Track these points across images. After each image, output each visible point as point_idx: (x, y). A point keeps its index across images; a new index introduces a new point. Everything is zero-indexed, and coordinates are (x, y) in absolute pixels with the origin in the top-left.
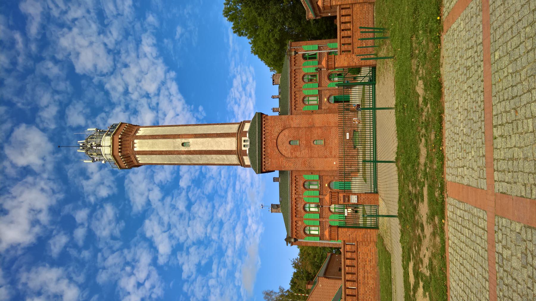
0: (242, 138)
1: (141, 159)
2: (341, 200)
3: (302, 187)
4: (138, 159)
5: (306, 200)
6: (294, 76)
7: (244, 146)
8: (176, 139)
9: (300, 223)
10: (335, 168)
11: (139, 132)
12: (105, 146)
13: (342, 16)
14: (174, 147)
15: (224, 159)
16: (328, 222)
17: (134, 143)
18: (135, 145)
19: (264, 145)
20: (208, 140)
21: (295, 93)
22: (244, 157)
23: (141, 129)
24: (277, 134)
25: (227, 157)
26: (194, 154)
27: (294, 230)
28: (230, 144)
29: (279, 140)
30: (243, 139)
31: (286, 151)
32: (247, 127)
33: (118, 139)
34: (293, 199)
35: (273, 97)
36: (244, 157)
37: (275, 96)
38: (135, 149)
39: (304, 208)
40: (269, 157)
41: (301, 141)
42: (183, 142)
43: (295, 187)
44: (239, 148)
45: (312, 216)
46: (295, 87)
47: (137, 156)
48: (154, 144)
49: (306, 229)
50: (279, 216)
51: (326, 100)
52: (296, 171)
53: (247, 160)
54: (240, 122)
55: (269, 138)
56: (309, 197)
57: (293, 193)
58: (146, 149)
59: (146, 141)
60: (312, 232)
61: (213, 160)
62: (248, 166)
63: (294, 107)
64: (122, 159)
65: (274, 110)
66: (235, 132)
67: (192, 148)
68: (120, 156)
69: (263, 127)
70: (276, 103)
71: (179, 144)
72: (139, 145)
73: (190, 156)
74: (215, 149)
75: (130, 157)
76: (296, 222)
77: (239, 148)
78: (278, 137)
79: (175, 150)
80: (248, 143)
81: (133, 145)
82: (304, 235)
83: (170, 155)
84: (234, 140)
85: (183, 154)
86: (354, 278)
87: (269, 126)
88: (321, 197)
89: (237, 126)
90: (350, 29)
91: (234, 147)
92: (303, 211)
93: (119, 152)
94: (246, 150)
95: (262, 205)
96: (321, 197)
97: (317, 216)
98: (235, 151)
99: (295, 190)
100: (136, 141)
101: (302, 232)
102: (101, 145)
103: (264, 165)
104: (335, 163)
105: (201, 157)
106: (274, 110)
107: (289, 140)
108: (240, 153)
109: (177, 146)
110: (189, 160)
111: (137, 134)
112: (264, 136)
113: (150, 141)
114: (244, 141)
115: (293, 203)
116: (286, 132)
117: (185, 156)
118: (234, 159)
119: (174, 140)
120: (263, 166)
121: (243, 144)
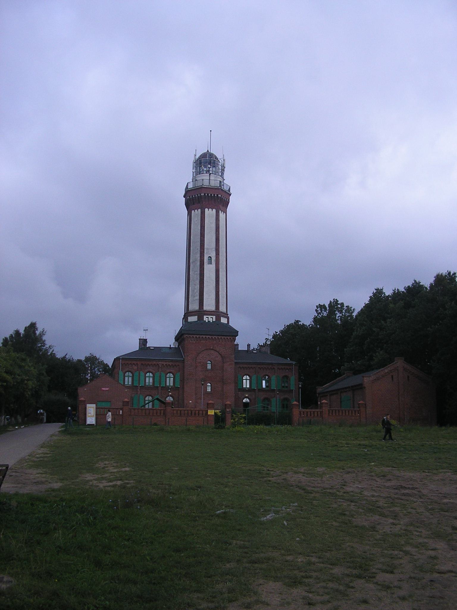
0: (215, 316)
1: (196, 213)
2: (228, 409)
3: (168, 371)
4: (196, 211)
5: (157, 375)
6: (269, 367)
8: (215, 251)
9: (136, 368)
10: (186, 401)
11: (222, 212)
13: (317, 412)
14: (208, 249)
15: (194, 297)
16: (137, 394)
18: (210, 210)
19: (209, 338)
20: (214, 283)
21: (254, 367)
23: (224, 214)
24: (218, 350)
25: (197, 299)
26: (200, 268)
27: (130, 362)
28: (209, 304)
29: (212, 352)
30: (214, 317)
31: (202, 357)
32: (224, 320)
33: (217, 194)
34: (157, 362)
35: (249, 346)
37: (250, 347)
38: (206, 210)
39: (149, 372)
40: (197, 341)
41: (211, 372)
42: (212, 258)
43: (169, 365)
44: (206, 313)
45: (142, 378)
46: (259, 368)
47: (199, 210)
48: (211, 229)
49: (130, 373)
50: (136, 347)
51: (247, 395)
52: (184, 367)
53: (193, 319)
54: (228, 313)
55: (215, 342)
56: (160, 377)
57: (163, 363)
59: (215, 221)
60: (126, 378)
61: (194, 285)
62: (185, 318)
63: (241, 366)
64: (198, 195)
66: (220, 309)
67: (206, 266)
68: (200, 194)
69: (224, 337)
71: (210, 254)
72: (210, 213)
73: (199, 263)
75: (199, 203)
77: (206, 313)
78: (216, 351)
79: (205, 250)
81: (210, 208)
82: (124, 371)
83: (200, 244)
84: (213, 308)
85: (201, 257)
86: (190, 415)
87: (225, 343)
88: (160, 388)
89: (225, 311)
90: (311, 416)
91: (205, 308)
92: (146, 371)
93: (205, 194)
95: (147, 330)
96: (160, 388)
97: (142, 384)
98: (203, 308)
99: (166, 365)
100: (214, 210)
101: (127, 369)
103: (190, 337)
104: (190, 402)
105: (196, 274)
107: (212, 360)
108: (201, 313)
109: (209, 252)
110: (194, 262)
111: (220, 211)
112: (216, 337)
113: (214, 226)
115: (154, 362)
116: (219, 358)
117: (199, 258)
118: (194, 307)
119: (214, 249)
120: (189, 336)
121: (210, 317)
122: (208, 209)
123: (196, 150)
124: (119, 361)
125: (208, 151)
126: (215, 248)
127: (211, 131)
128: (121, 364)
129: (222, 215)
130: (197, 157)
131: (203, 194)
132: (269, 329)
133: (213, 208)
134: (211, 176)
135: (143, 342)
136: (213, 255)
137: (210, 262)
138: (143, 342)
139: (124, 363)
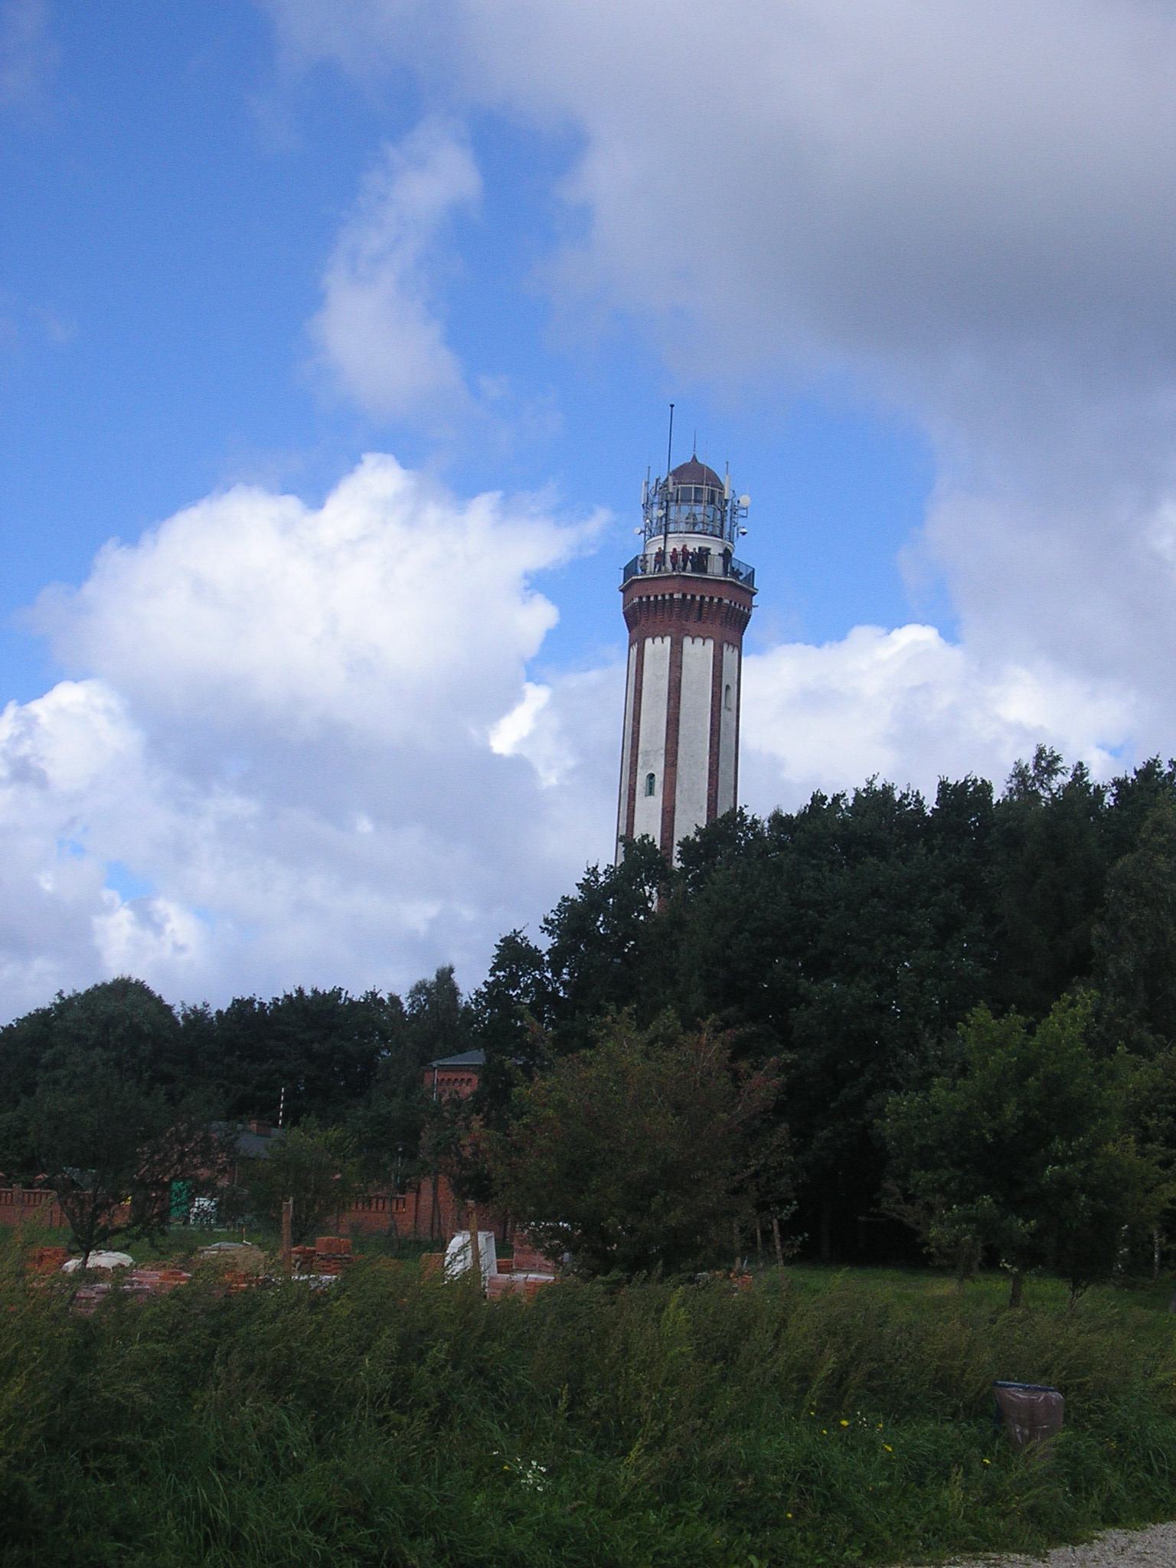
8: (664, 756)
14: (647, 753)
27: (453, 1076)
33: (671, 591)
38: (648, 642)
76: (470, 1080)
79: (640, 757)
81: (657, 636)
102: (670, 536)
109: (649, 760)
111: (687, 641)
113: (664, 685)
119: (663, 751)
122: (662, 638)
123: (649, 467)
124: (432, 1074)
125: (694, 458)
126: (664, 747)
127: (672, 406)
128: (437, 1080)
131: (637, 599)
133: (665, 635)
134: (668, 540)
136: (659, 769)
139: (443, 1080)
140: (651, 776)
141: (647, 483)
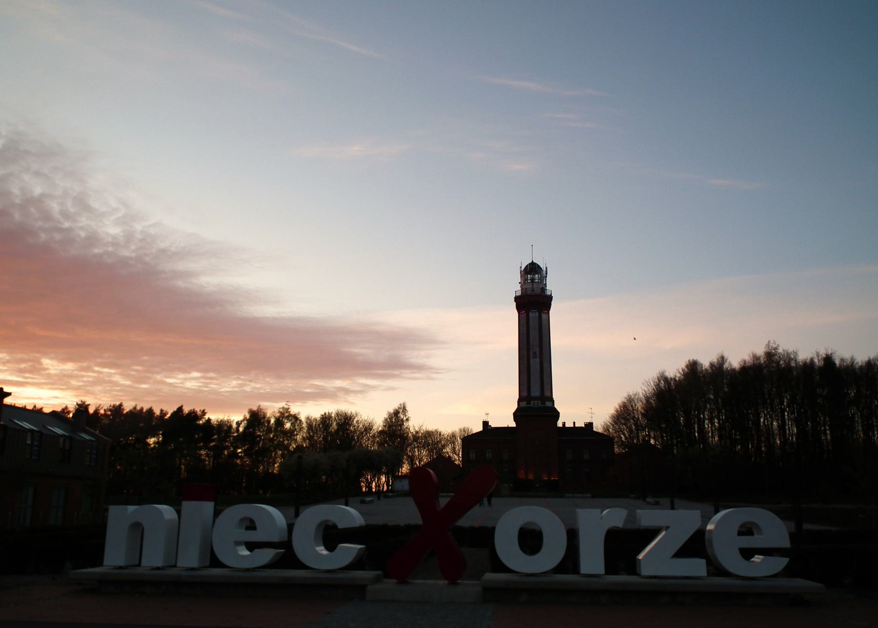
7: (534, 403)
11: (545, 314)
12: (533, 288)
17: (535, 312)
22: (525, 402)
23: (547, 315)
28: (535, 392)
30: (540, 402)
32: (548, 404)
35: (574, 423)
36: (525, 402)
38: (530, 313)
58: (531, 322)
65: (564, 424)
67: (532, 361)
70: (569, 424)
72: (534, 315)
74: (532, 379)
80: (536, 406)
94: (530, 404)
100: (537, 313)
106: (564, 424)
111: (542, 314)
114: (538, 403)
121: (536, 402)
125: (533, 261)
129: (544, 316)
130: (523, 268)
132: (591, 409)
135: (485, 424)
136: (537, 350)
137: (535, 357)
138: (485, 424)
140: (535, 353)
141: (521, 267)
